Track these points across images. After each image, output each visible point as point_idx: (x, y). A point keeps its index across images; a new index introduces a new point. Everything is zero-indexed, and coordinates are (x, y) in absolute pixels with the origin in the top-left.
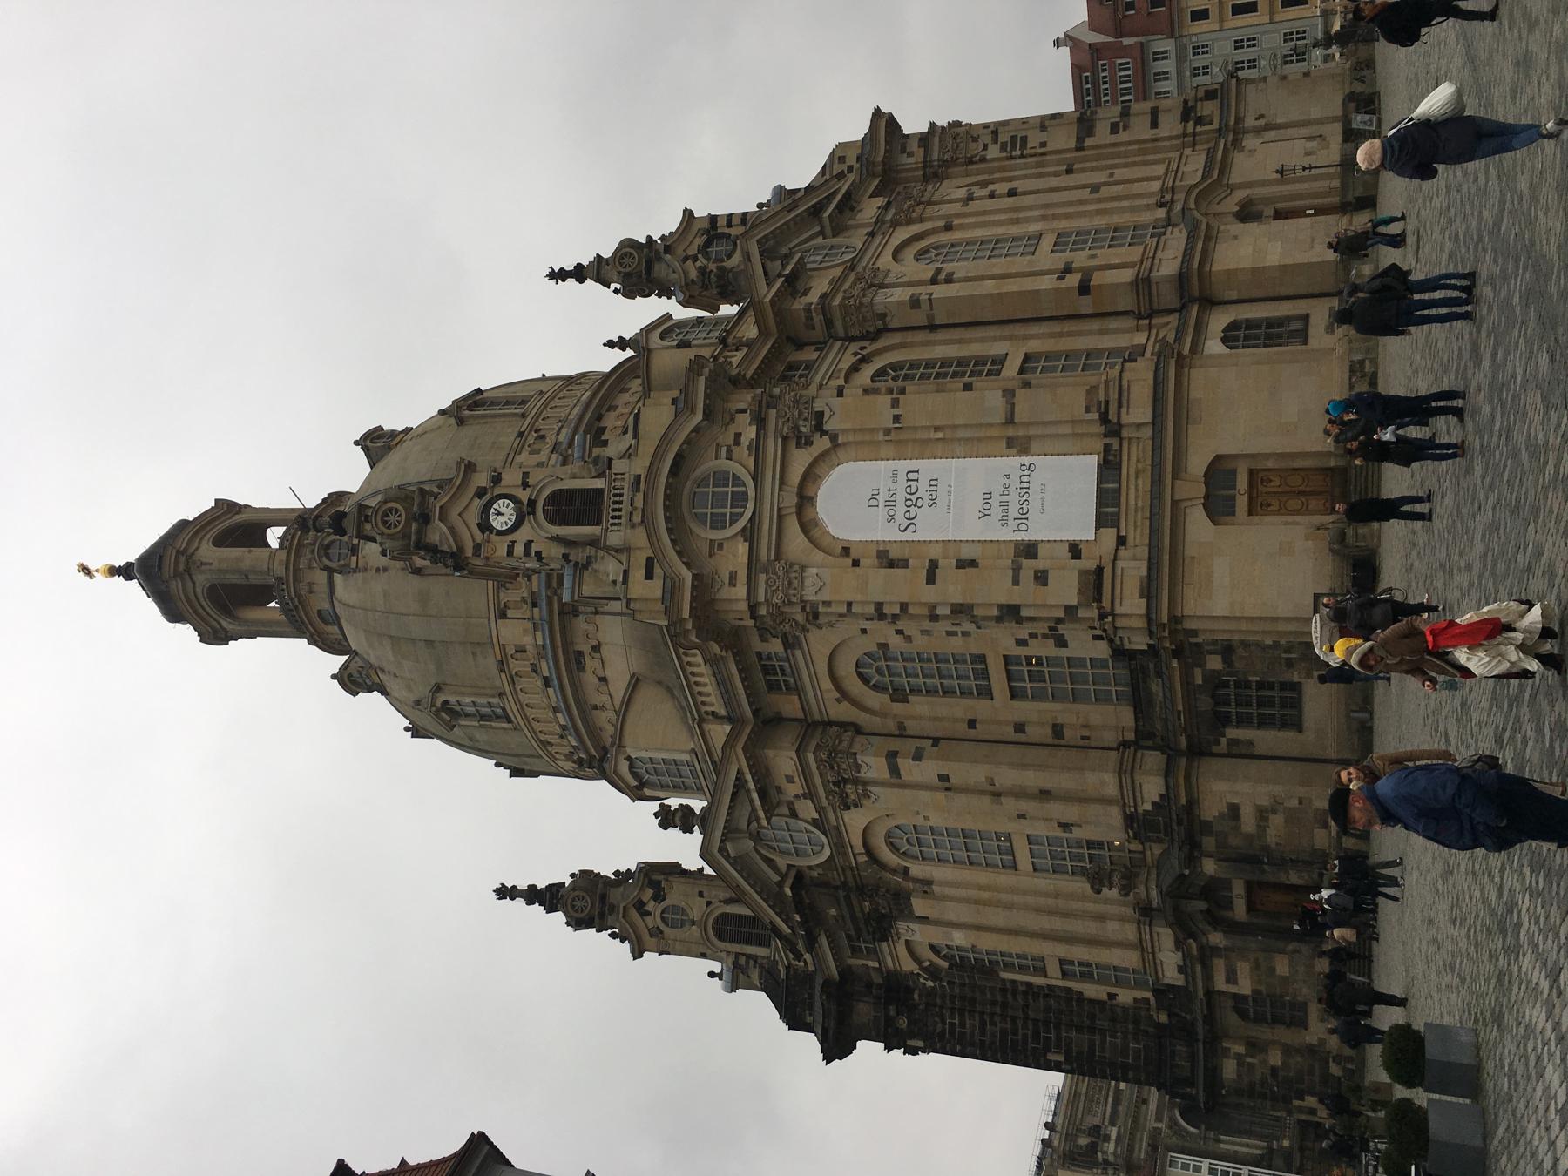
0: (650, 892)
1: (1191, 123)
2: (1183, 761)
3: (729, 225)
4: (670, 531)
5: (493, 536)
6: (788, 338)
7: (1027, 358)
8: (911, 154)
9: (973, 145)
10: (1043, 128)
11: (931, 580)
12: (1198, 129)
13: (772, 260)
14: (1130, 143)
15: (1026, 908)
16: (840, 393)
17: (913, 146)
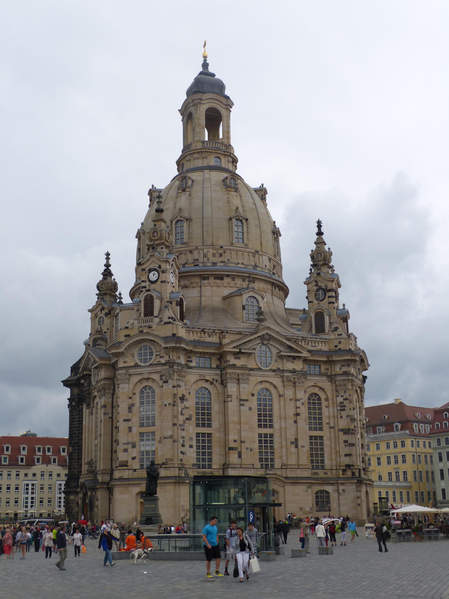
0: (107, 311)
1: (344, 468)
2: (105, 486)
3: (329, 297)
4: (134, 342)
5: (147, 274)
6: (221, 355)
7: (210, 435)
8: (340, 369)
9: (343, 391)
10: (347, 416)
11: (125, 420)
12: (341, 471)
13: (261, 339)
14: (339, 447)
15: (88, 443)
16: (174, 387)
17: (344, 369)
